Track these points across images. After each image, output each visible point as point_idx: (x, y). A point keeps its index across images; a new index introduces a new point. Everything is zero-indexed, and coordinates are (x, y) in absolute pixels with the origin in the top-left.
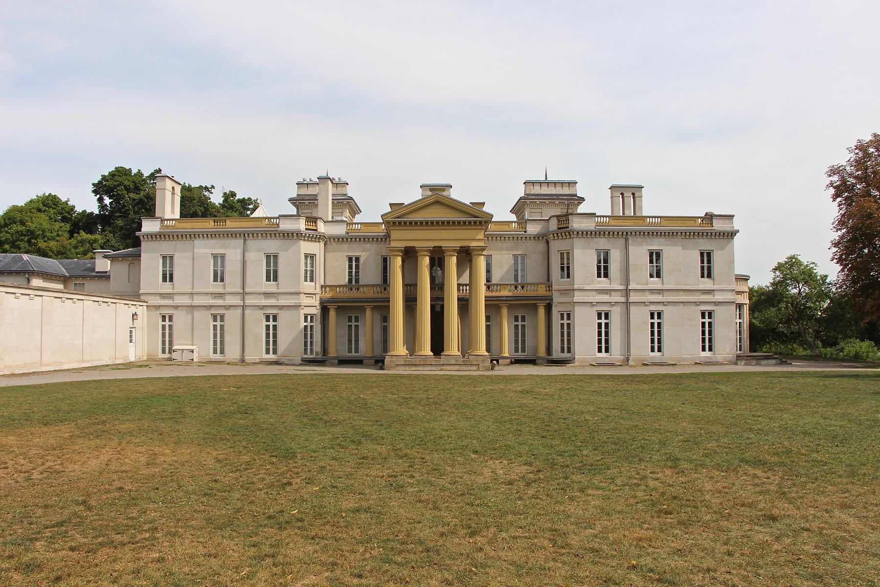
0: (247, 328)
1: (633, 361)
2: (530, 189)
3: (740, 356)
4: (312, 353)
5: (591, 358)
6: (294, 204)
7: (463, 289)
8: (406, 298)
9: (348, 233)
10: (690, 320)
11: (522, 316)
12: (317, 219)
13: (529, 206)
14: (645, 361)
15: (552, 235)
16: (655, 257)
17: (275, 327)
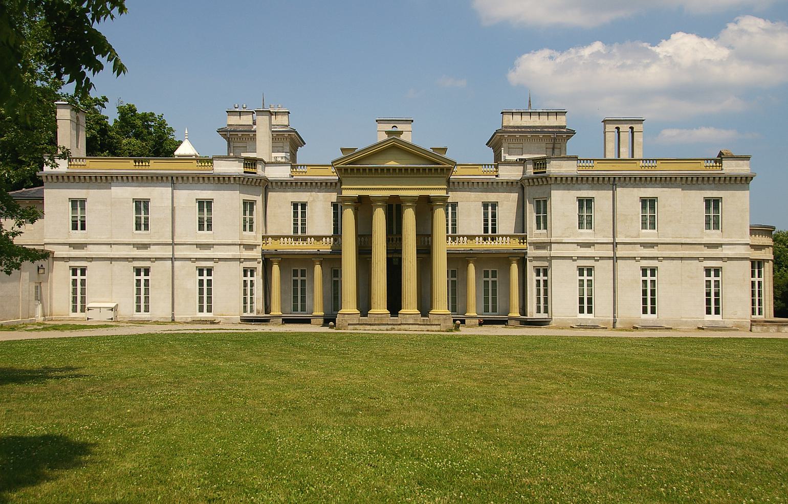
0: (176, 282)
1: (621, 323)
2: (509, 120)
3: (755, 321)
4: (252, 311)
5: (572, 319)
6: (224, 136)
7: (424, 241)
8: (359, 250)
9: (293, 176)
10: (692, 278)
12: (257, 160)
13: (507, 140)
14: (634, 324)
15: (526, 181)
16: (649, 203)
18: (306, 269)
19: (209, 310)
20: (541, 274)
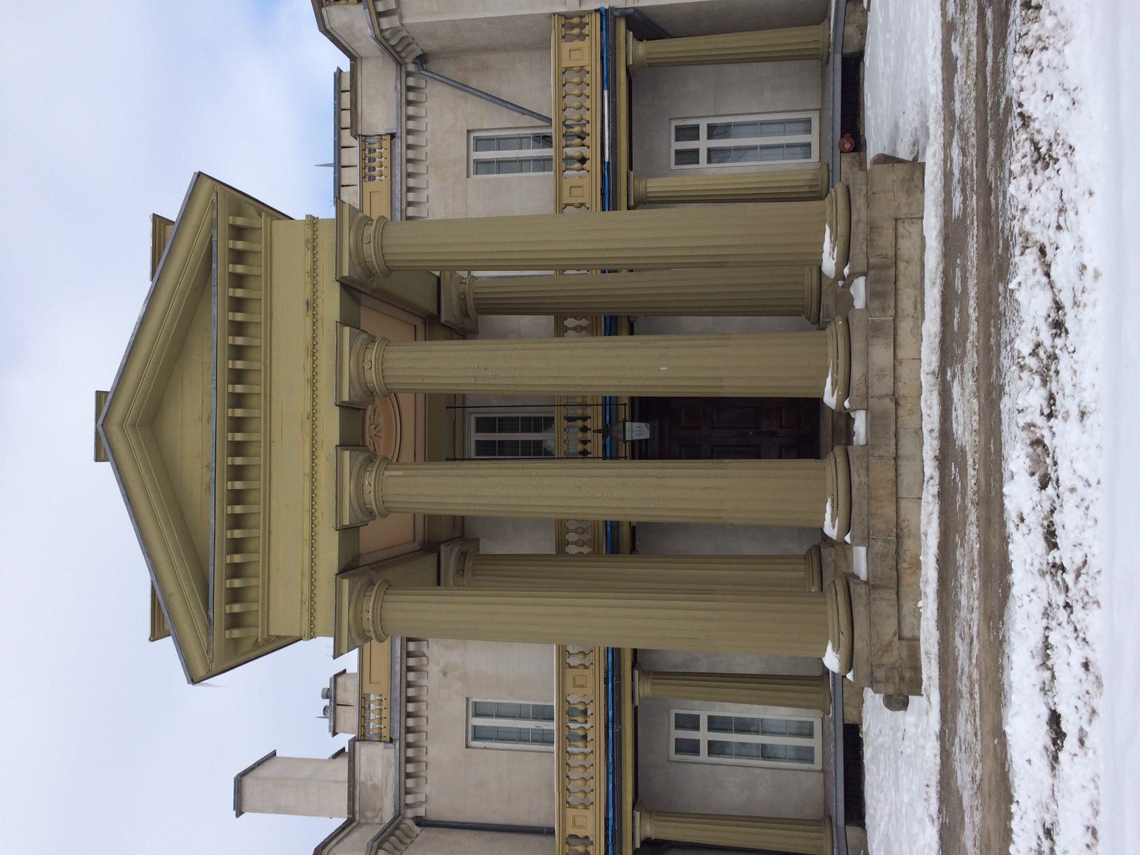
11: (677, 139)
15: (385, 23)
18: (673, 712)
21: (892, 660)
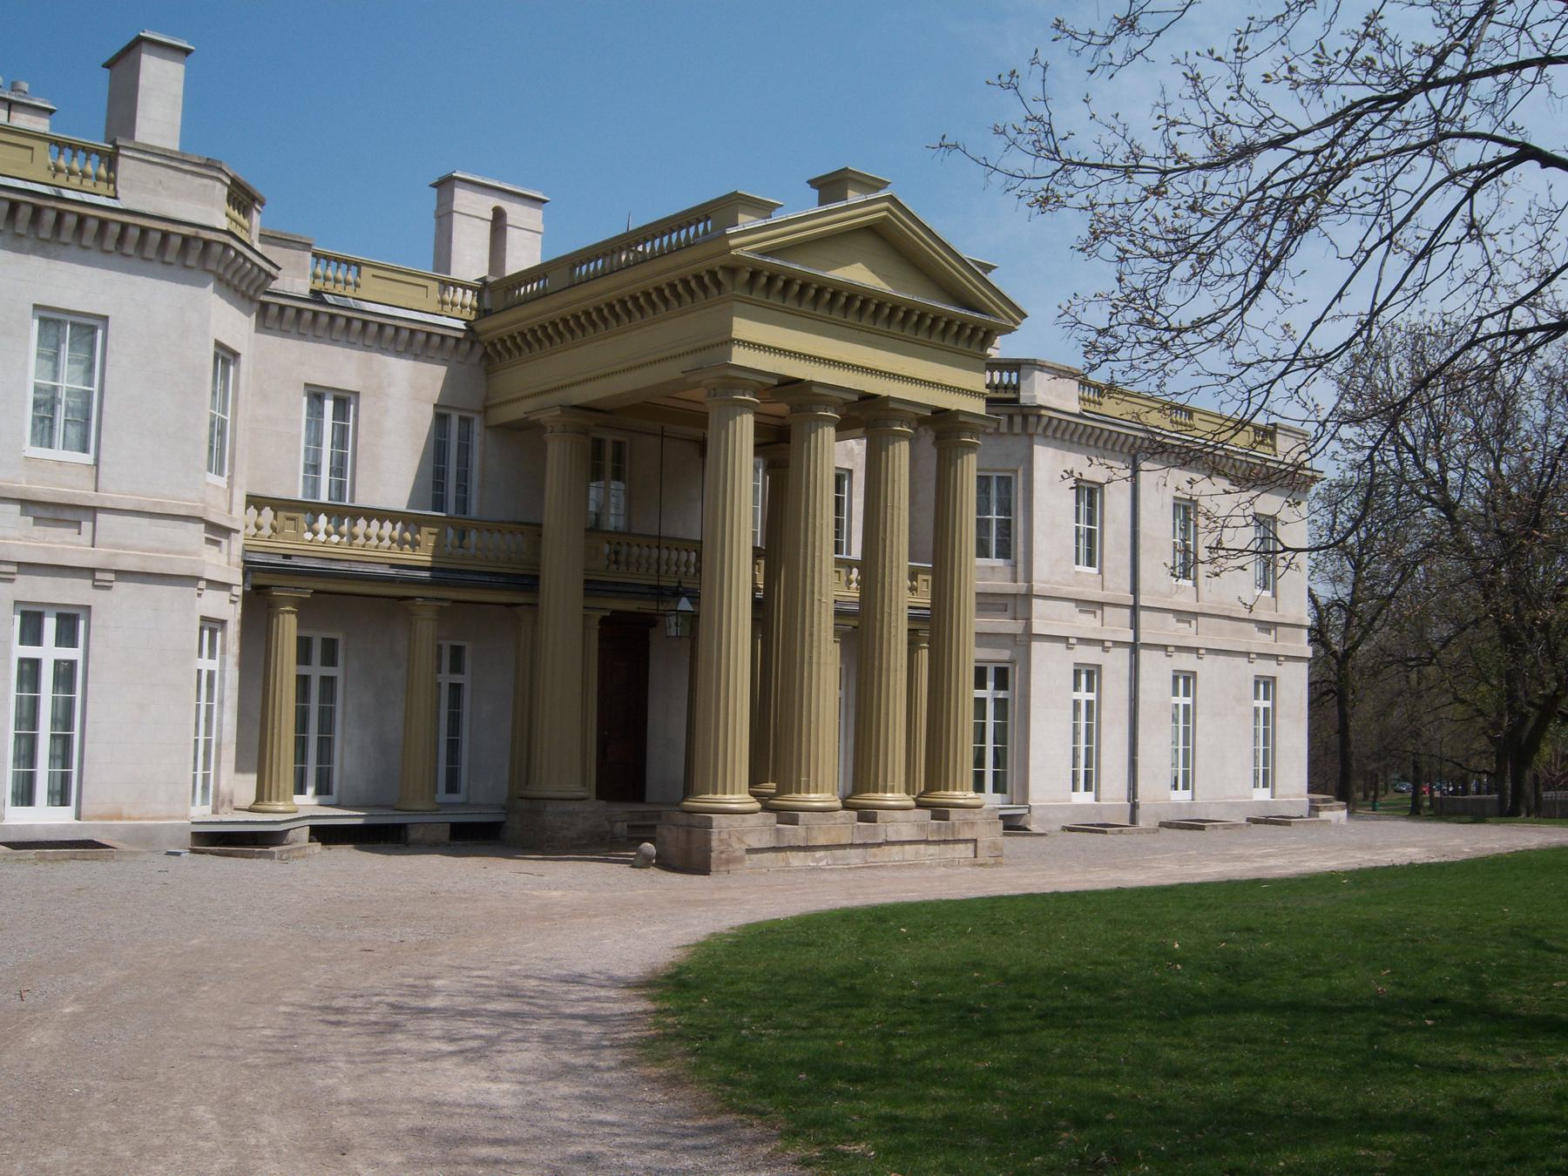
17: (65, 674)
19: (61, 795)
20: (990, 684)
21: (733, 845)
